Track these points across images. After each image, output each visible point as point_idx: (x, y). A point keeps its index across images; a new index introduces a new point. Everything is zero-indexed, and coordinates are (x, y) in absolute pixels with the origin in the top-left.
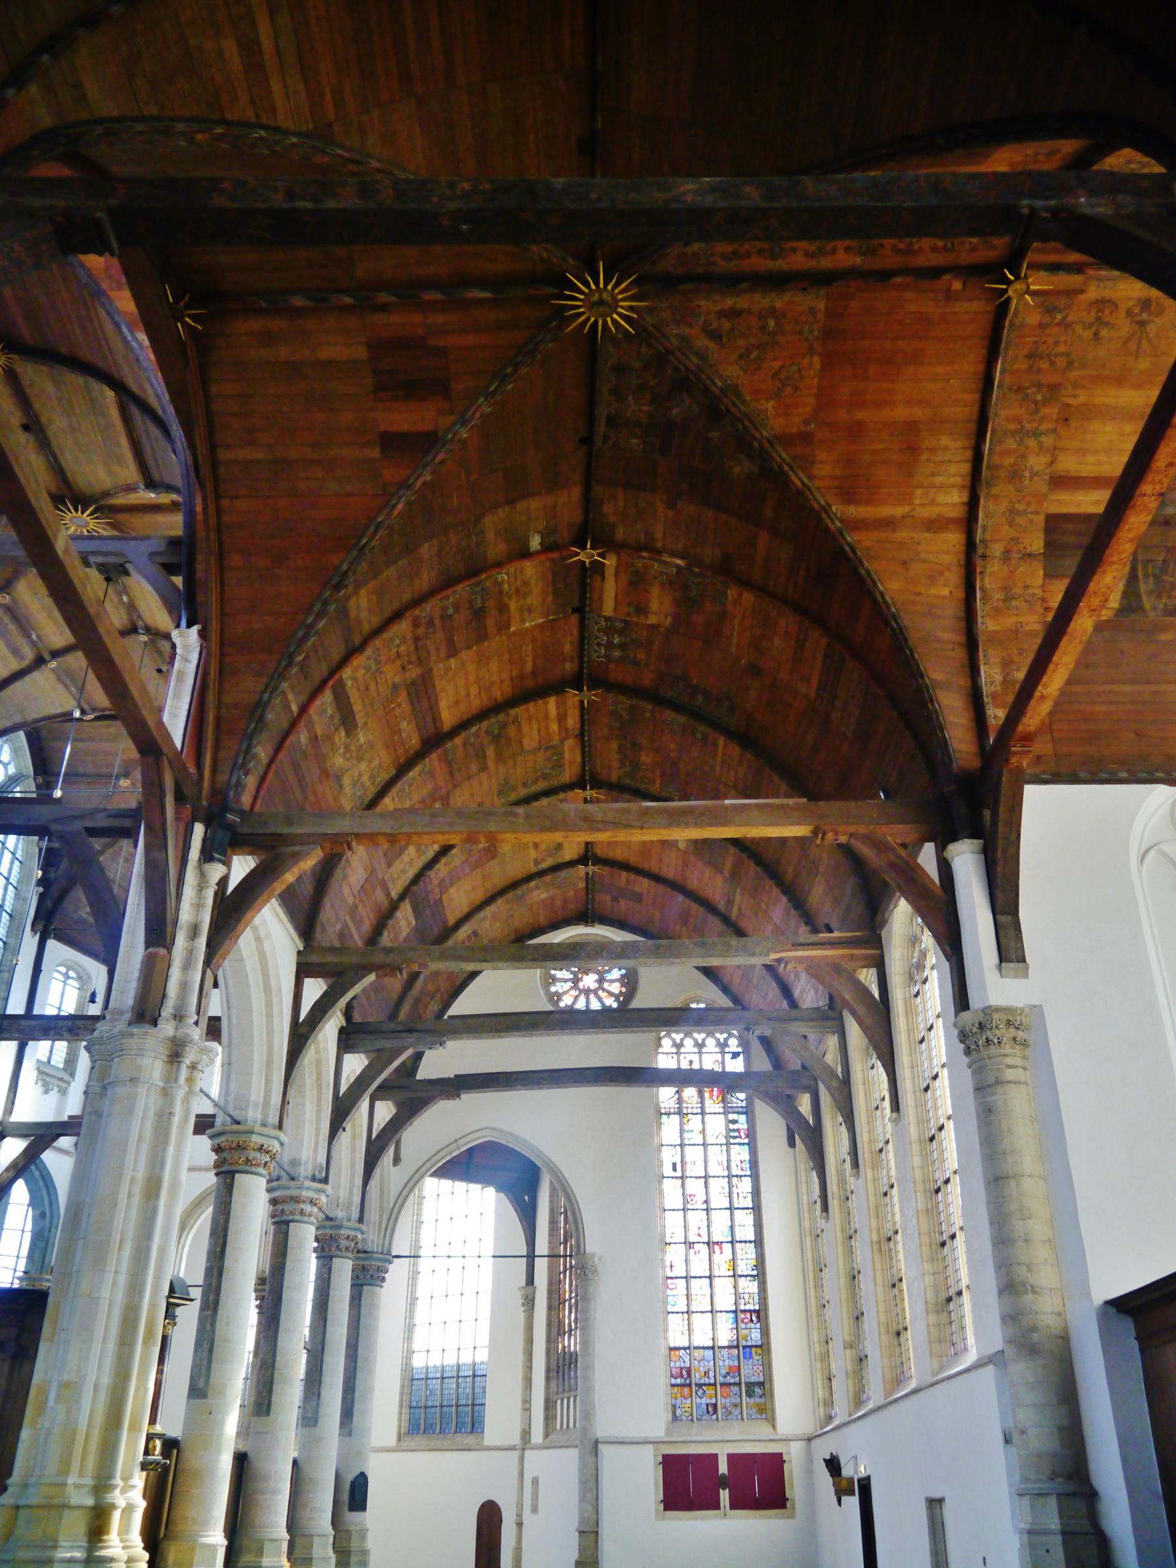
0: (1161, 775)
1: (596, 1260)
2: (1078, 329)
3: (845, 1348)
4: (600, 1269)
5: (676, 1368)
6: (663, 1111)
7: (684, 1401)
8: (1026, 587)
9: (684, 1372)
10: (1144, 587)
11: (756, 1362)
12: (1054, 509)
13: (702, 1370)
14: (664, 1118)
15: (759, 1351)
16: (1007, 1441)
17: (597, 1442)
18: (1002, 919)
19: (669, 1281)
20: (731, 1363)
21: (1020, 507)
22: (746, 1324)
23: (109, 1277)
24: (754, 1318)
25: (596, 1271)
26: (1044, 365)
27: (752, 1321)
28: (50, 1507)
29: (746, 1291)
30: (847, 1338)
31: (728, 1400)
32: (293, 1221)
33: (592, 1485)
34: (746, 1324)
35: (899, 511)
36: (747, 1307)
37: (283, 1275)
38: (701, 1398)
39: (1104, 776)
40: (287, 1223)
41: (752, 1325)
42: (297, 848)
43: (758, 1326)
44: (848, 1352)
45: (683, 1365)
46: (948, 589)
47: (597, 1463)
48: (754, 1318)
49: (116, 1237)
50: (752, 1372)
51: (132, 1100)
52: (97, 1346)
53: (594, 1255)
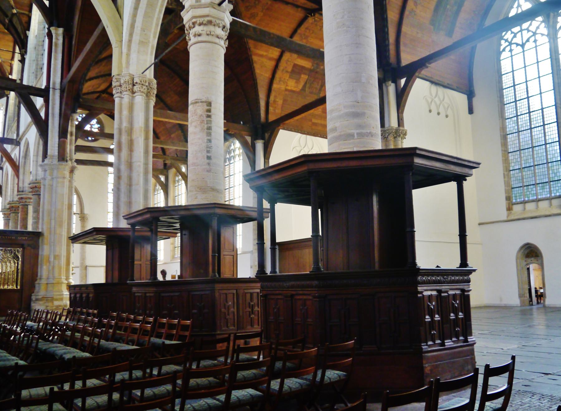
0: (300, 131)
1: (88, 215)
2: (318, 26)
3: (171, 244)
4: (88, 218)
6: (109, 172)
8: (285, 79)
10: (308, 86)
12: (296, 63)
14: (110, 175)
16: (251, 267)
17: (86, 267)
18: (266, 160)
19: (109, 223)
21: (290, 60)
23: (64, 229)
25: (87, 219)
26: (308, 31)
28: (58, 283)
30: (172, 242)
32: (30, 205)
33: (85, 278)
35: (265, 54)
37: (27, 221)
39: (289, 129)
40: (27, 205)
42: (97, 112)
44: (172, 245)
46: (268, 75)
47: (86, 272)
49: (64, 220)
51: (63, 182)
52: (63, 246)
53: (87, 214)
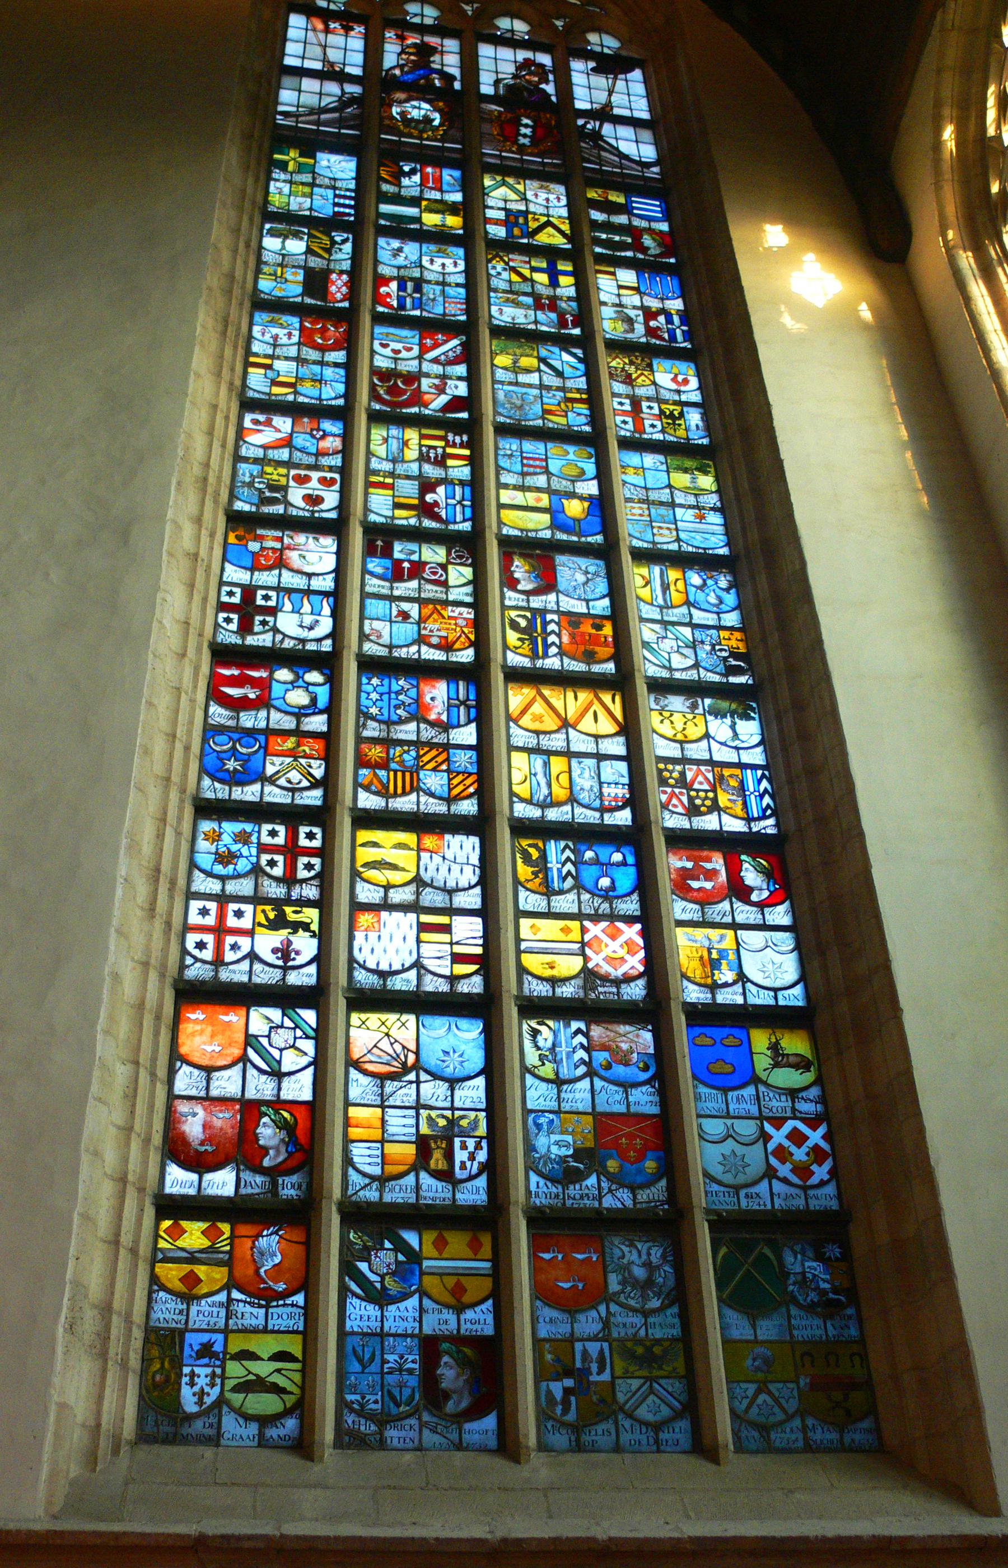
5: (208, 1100)
7: (251, 1315)
9: (267, 1133)
11: (778, 1104)
13: (400, 1124)
15: (795, 1044)
20: (611, 1099)
22: (704, 900)
24: (751, 876)
27: (739, 891)
29: (697, 751)
31: (588, 1323)
34: (704, 900)
36: (709, 822)
38: (380, 1298)
41: (745, 914)
43: (780, 915)
45: (261, 1087)
48: (751, 876)
50: (755, 1155)
